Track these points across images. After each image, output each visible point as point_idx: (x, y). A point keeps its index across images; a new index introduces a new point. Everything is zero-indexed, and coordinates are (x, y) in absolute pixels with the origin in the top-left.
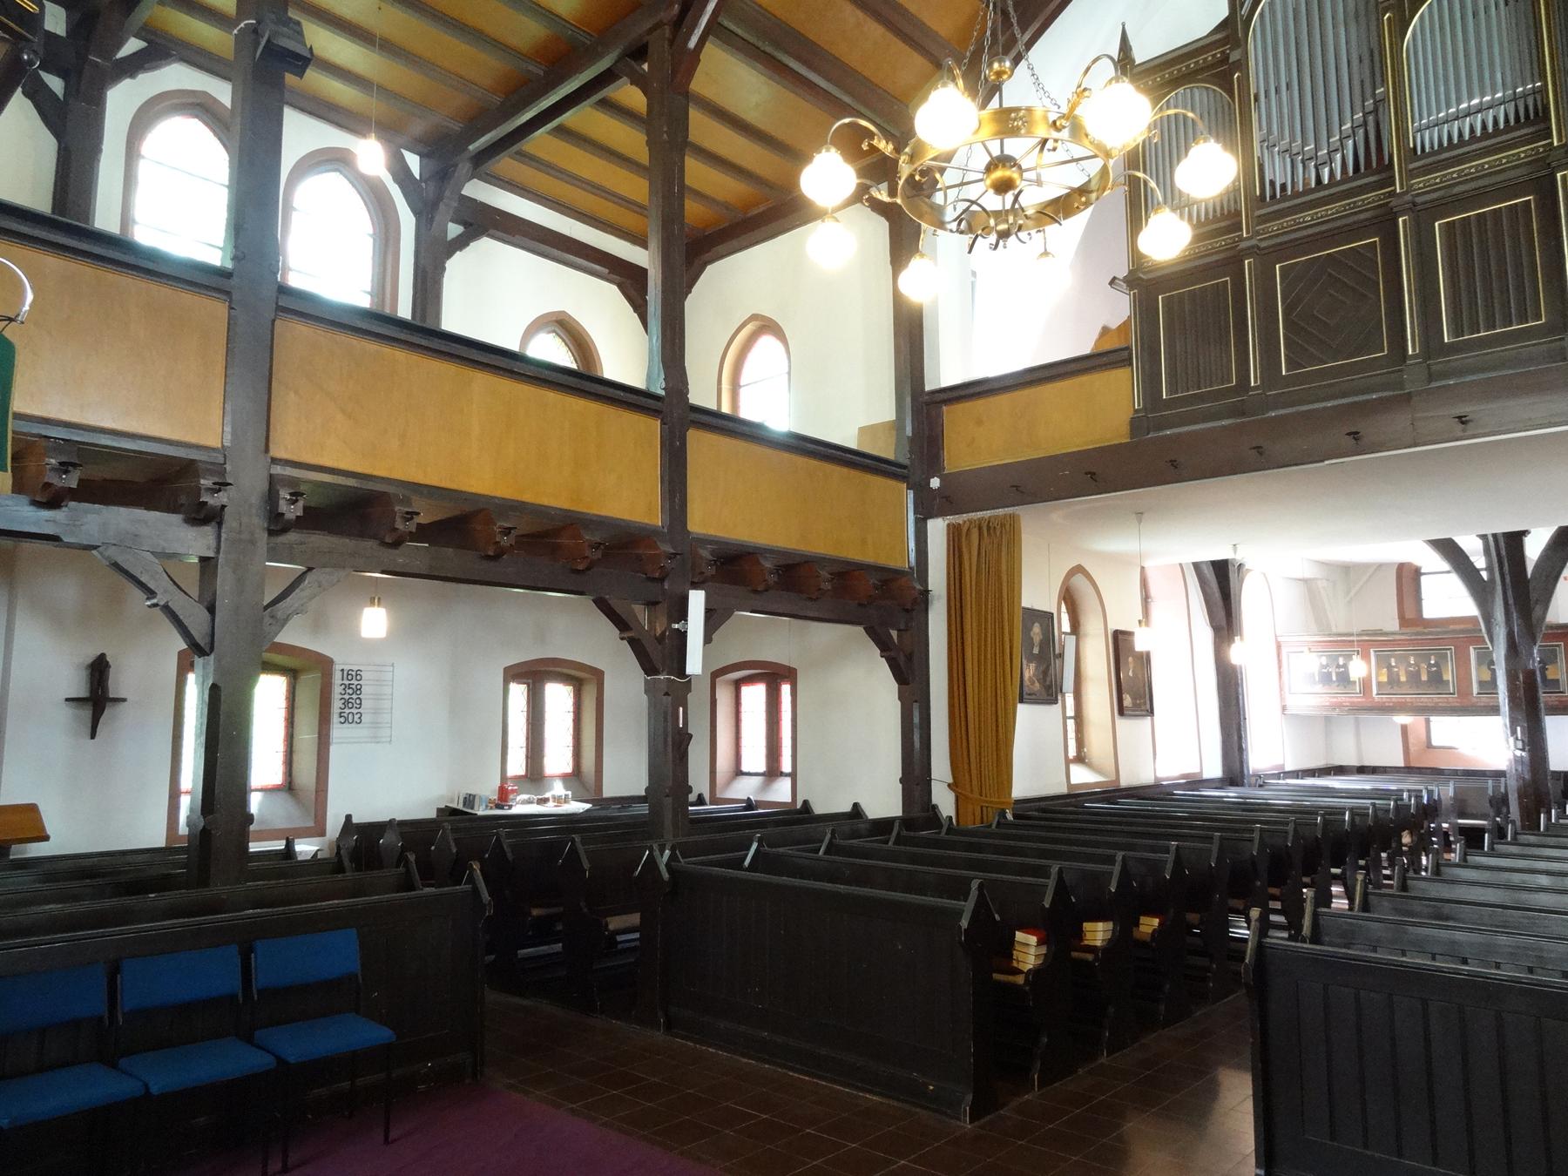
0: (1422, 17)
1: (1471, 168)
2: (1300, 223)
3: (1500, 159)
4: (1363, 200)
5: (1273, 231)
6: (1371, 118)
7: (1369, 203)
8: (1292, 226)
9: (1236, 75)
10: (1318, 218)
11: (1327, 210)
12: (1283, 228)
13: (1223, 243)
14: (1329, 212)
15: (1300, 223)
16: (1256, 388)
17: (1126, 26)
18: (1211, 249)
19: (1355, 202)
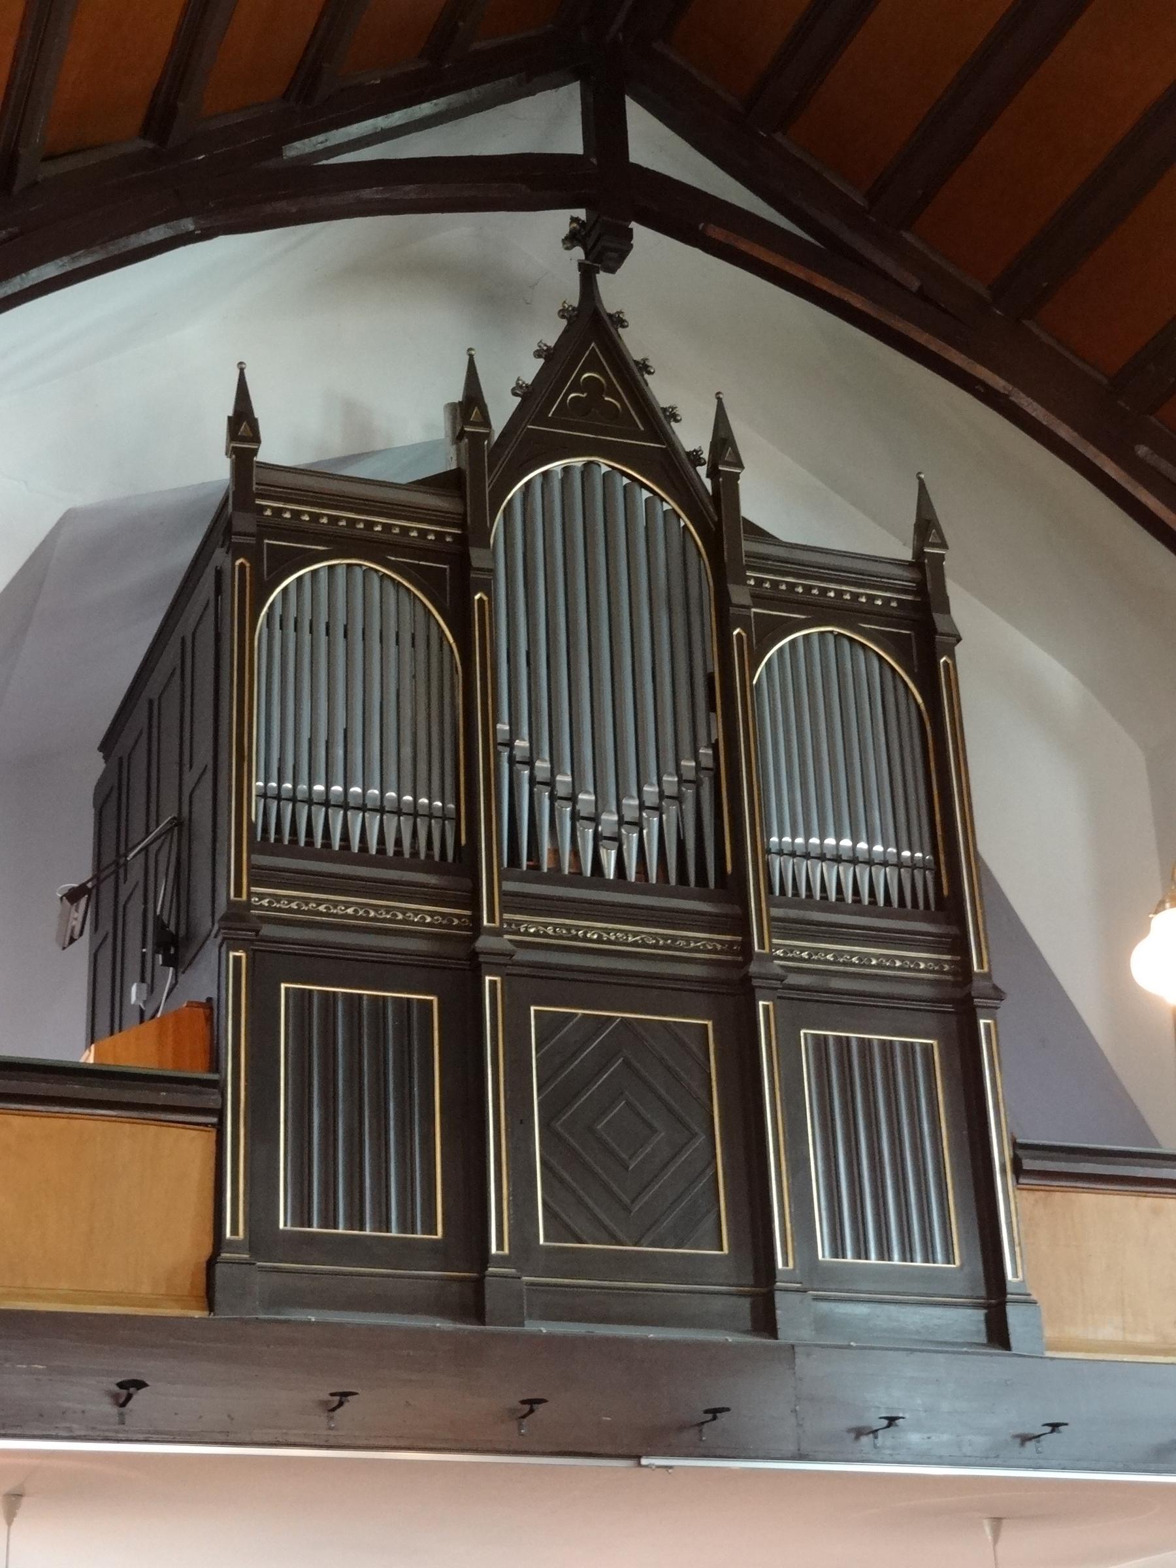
0: (769, 665)
1: (852, 954)
2: (576, 938)
3: (892, 958)
4: (688, 940)
5: (527, 933)
6: (689, 792)
7: (696, 950)
8: (561, 937)
9: (477, 597)
10: (609, 942)
11: (626, 932)
12: (546, 935)
13: (428, 920)
14: (630, 939)
15: (576, 938)
16: (502, 1261)
17: (246, 371)
18: (400, 922)
19: (674, 938)
